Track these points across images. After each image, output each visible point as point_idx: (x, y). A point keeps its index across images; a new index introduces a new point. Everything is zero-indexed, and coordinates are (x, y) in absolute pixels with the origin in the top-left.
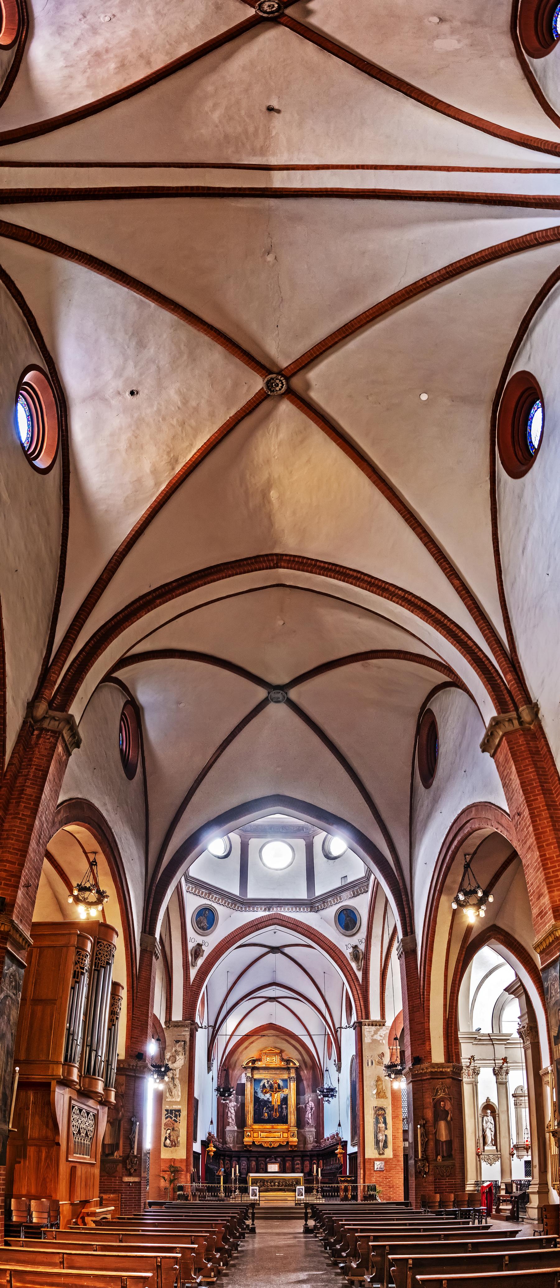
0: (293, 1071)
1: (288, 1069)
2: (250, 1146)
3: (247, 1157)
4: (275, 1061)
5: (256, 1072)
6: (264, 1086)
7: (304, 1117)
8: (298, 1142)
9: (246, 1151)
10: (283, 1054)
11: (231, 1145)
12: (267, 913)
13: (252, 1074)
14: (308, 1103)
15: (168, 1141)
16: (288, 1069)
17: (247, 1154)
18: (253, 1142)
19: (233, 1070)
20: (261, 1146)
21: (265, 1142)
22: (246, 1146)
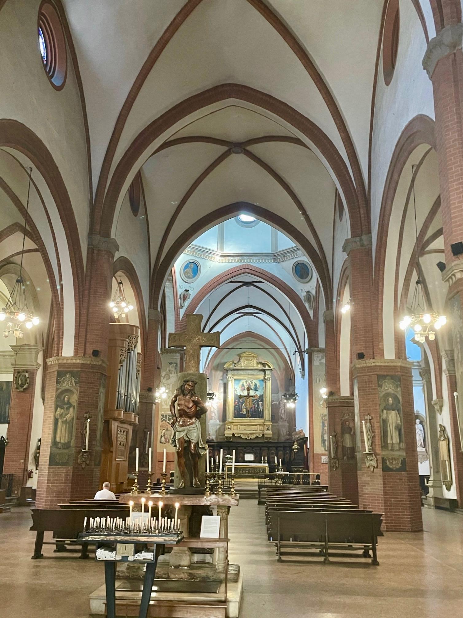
8: (273, 434)
12: (239, 264)
15: (163, 438)
18: (233, 434)
21: (244, 434)
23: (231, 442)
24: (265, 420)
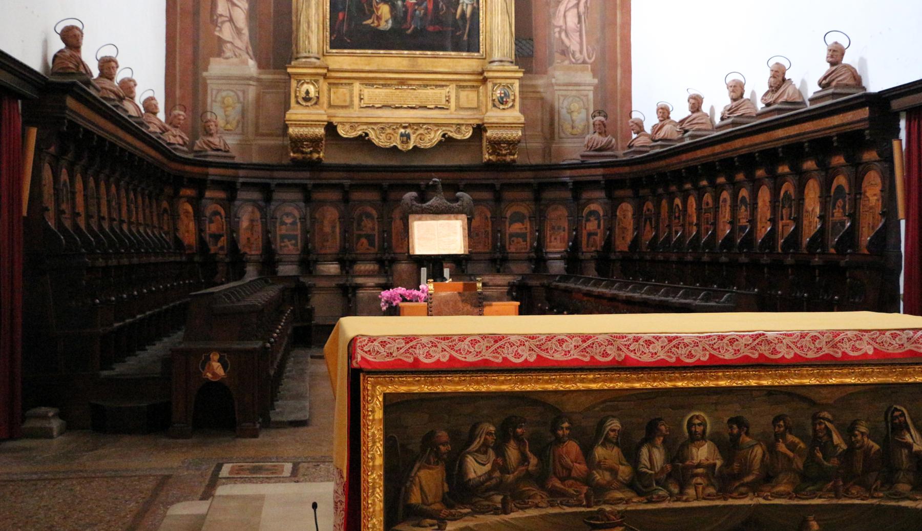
2: (315, 142)
3: (303, 188)
7: (548, 23)
8: (525, 127)
9: (297, 165)
11: (231, 141)
17: (304, 177)
18: (331, 128)
20: (363, 142)
22: (297, 143)
23: (316, 166)
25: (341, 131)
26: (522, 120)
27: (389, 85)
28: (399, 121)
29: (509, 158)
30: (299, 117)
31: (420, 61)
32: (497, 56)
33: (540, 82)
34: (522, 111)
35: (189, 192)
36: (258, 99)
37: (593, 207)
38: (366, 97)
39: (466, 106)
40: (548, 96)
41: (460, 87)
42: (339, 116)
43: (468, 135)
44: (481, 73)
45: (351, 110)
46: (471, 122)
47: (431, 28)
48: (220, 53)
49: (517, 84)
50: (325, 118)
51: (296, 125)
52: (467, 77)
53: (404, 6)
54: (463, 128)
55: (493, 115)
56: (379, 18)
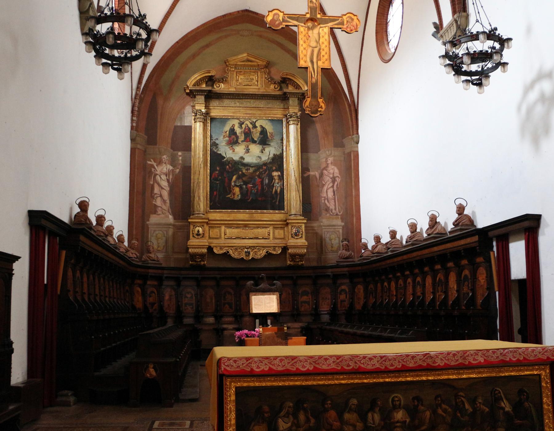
0: (293, 103)
1: (284, 98)
2: (202, 256)
3: (196, 279)
4: (256, 83)
5: (214, 103)
6: (232, 131)
7: (319, 196)
8: (308, 247)
10: (273, 70)
11: (160, 256)
13: (207, 107)
14: (326, 168)
16: (284, 98)
18: (210, 249)
19: (167, 99)
20: (226, 255)
21: (236, 248)
22: (193, 256)
23: (203, 268)
24: (288, 214)
25: (215, 251)
26: (307, 244)
27: (239, 227)
28: (244, 245)
29: (300, 263)
30: (194, 244)
31: (255, 215)
32: (293, 212)
33: (315, 224)
34: (306, 239)
35: (139, 281)
36: (174, 234)
37: (343, 287)
38: (228, 234)
39: (278, 237)
40: (319, 232)
41: (275, 228)
42: (214, 243)
43: (279, 252)
44: (286, 221)
45: (220, 240)
46: (281, 245)
47: (260, 199)
48: (155, 212)
49: (303, 226)
50: (207, 244)
51: (193, 248)
52: (278, 223)
53: (246, 188)
54: (277, 248)
55: (292, 242)
56: (234, 194)
